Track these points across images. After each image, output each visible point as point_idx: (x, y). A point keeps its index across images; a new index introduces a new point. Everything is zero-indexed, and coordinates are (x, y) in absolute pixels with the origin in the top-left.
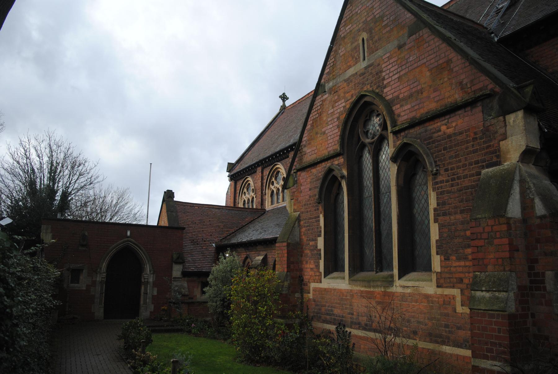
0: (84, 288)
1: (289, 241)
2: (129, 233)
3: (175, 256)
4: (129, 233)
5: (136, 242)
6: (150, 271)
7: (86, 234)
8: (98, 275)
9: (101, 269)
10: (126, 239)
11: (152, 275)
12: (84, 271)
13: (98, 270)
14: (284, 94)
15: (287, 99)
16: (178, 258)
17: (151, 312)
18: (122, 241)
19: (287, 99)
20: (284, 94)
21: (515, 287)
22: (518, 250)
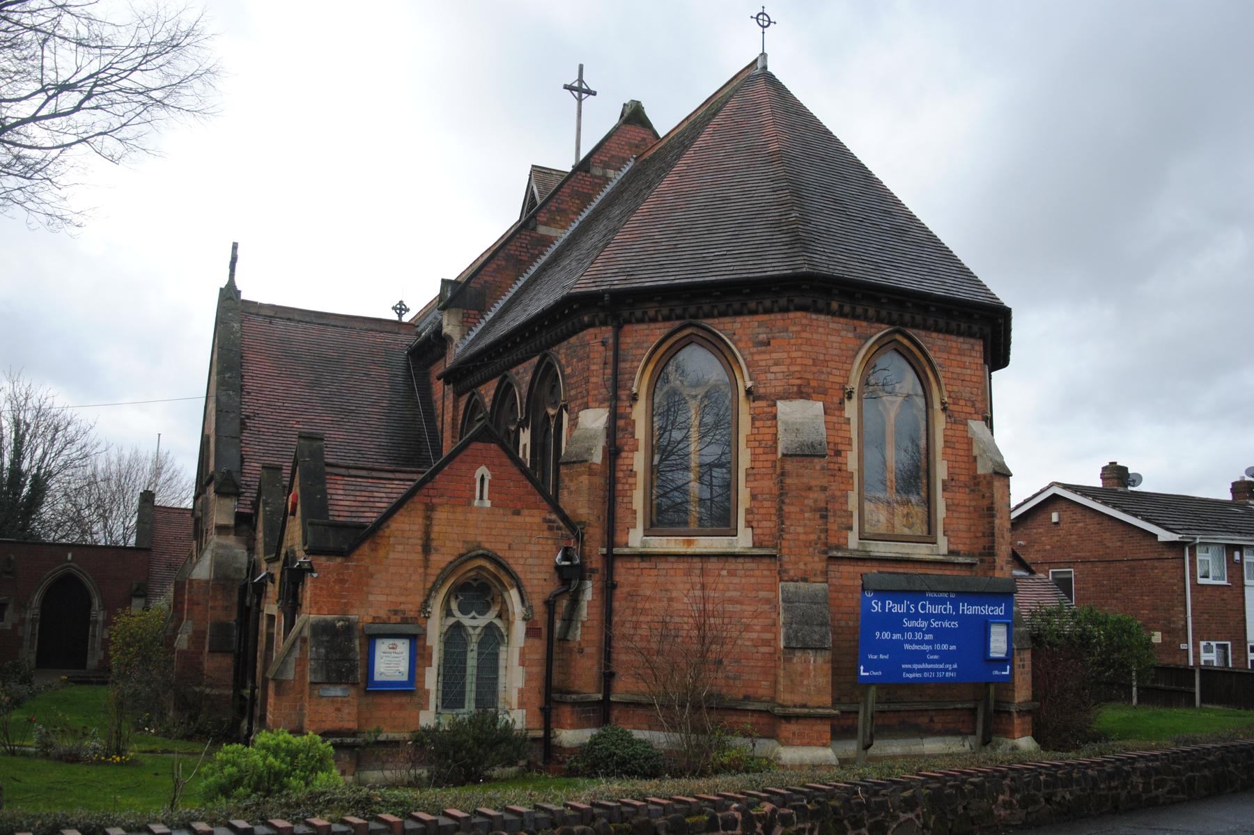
0: (10, 628)
1: (178, 579)
2: (70, 556)
3: (134, 587)
4: (70, 556)
5: (79, 568)
6: (99, 606)
7: (13, 557)
8: (28, 611)
9: (31, 603)
10: (67, 564)
11: (102, 612)
12: (10, 606)
13: (28, 605)
14: (401, 303)
15: (407, 310)
16: (138, 589)
17: (100, 661)
18: (59, 567)
19: (407, 310)
20: (401, 303)
21: (190, 632)
22: (198, 604)
